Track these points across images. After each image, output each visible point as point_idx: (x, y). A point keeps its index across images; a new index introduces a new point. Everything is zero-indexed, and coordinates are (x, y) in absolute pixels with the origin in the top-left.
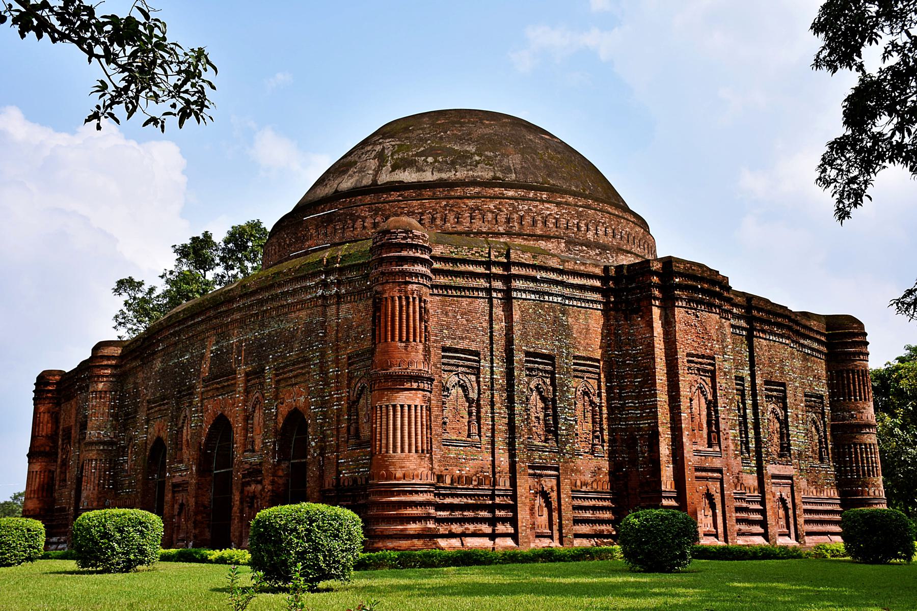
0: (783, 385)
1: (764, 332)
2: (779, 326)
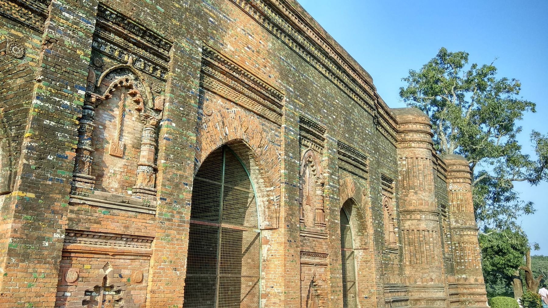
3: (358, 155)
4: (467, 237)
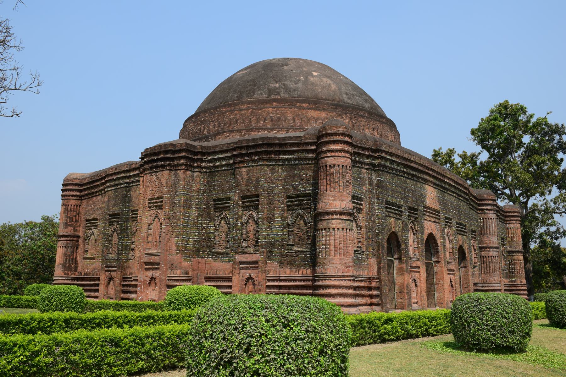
0: (257, 196)
1: (241, 162)
2: (256, 154)
3: (463, 225)
4: (516, 256)
